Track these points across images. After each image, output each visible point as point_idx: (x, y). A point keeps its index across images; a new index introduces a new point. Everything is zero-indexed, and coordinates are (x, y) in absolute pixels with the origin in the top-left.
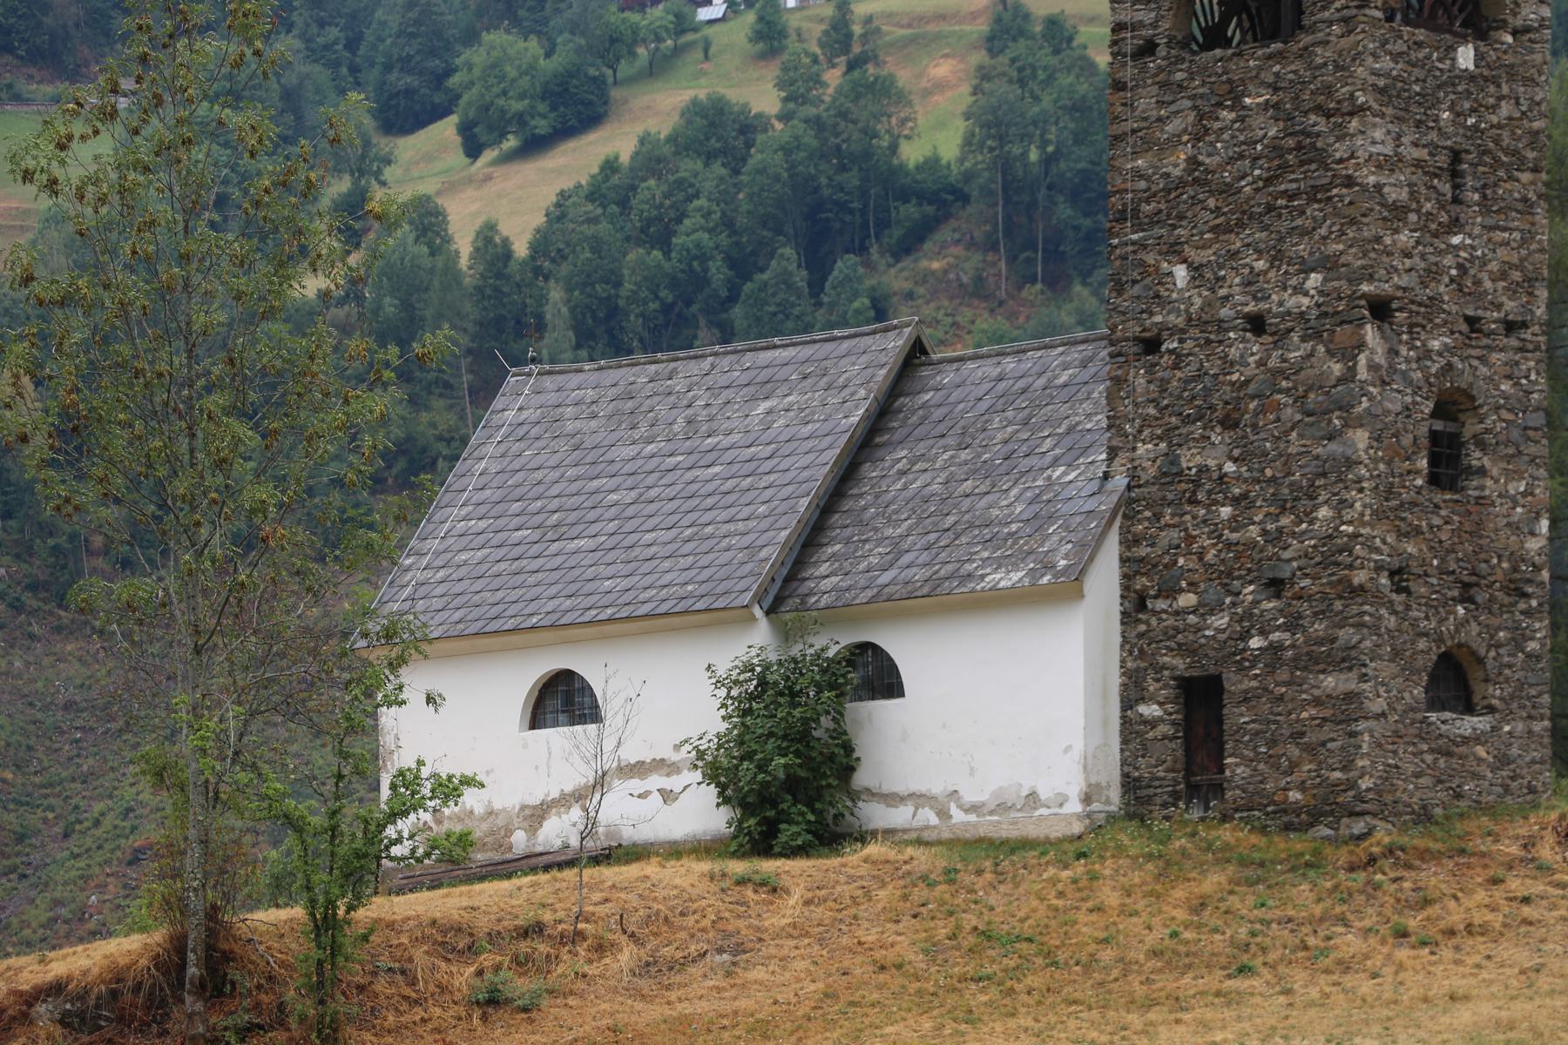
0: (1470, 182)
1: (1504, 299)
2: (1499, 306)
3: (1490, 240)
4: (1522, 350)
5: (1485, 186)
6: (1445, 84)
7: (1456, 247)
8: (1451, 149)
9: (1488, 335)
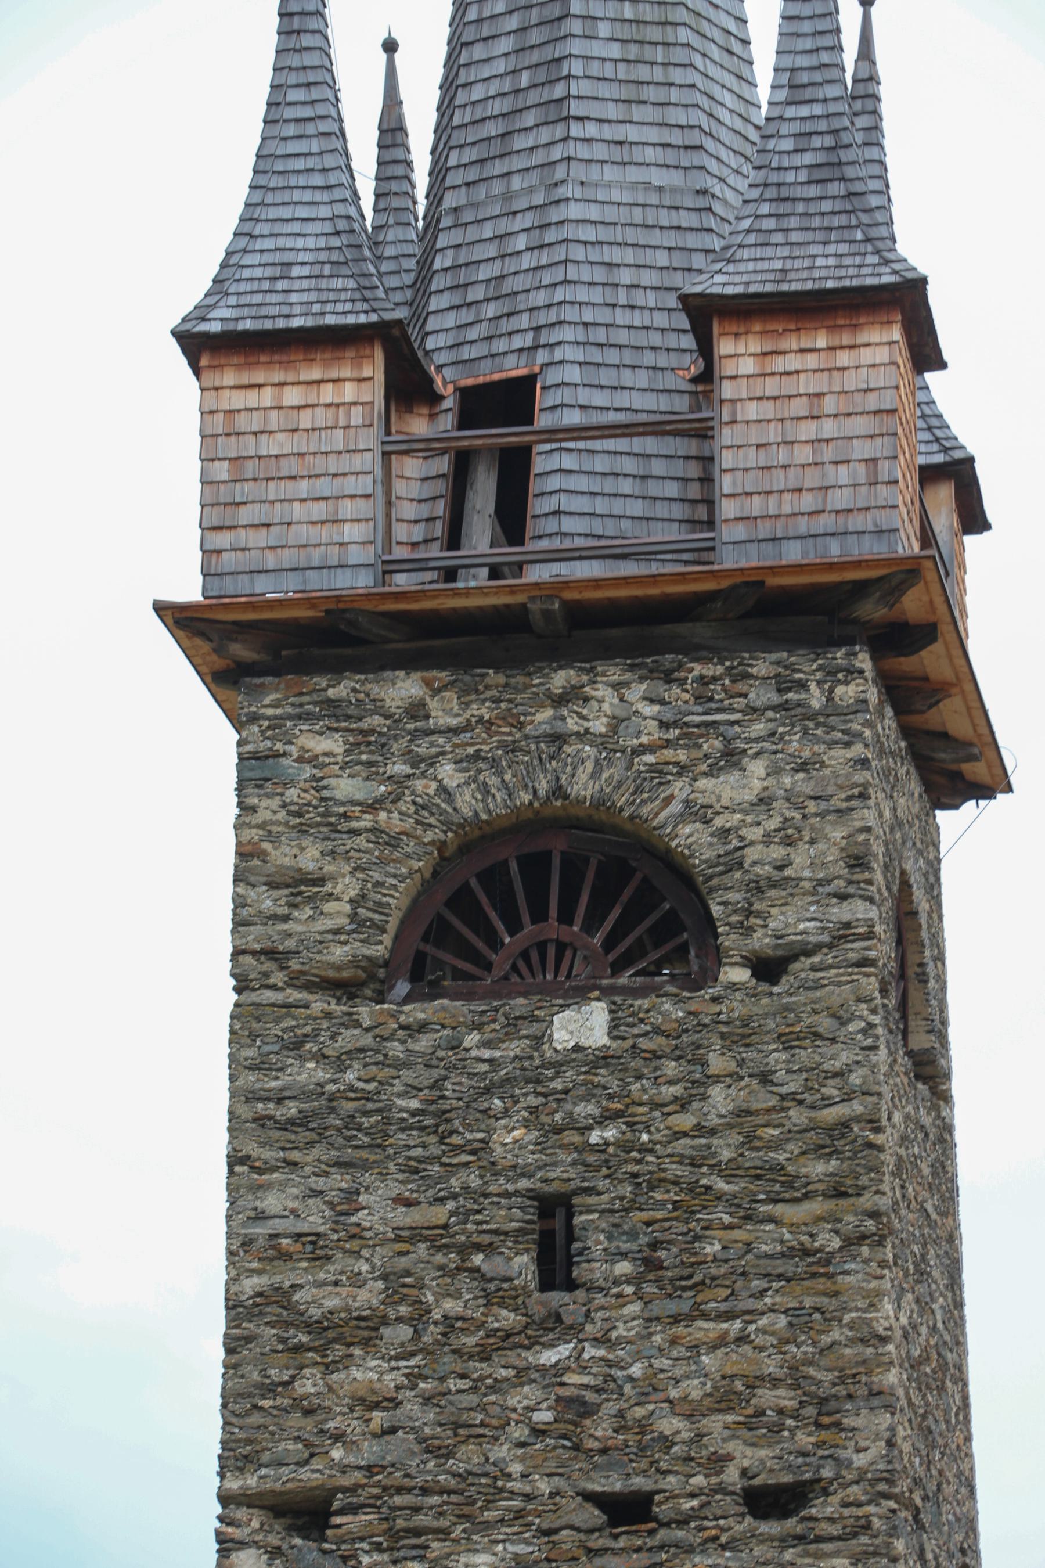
0: (597, 1243)
1: (731, 1447)
2: (718, 1462)
3: (674, 1342)
4: (801, 1538)
5: (654, 1245)
6: (507, 1080)
7: (559, 1369)
8: (532, 1195)
9: (683, 1522)
